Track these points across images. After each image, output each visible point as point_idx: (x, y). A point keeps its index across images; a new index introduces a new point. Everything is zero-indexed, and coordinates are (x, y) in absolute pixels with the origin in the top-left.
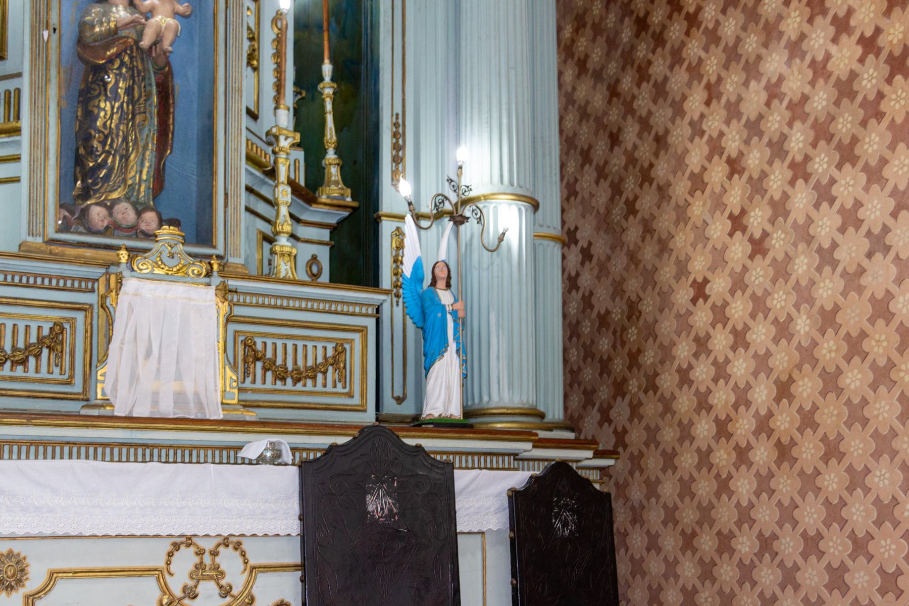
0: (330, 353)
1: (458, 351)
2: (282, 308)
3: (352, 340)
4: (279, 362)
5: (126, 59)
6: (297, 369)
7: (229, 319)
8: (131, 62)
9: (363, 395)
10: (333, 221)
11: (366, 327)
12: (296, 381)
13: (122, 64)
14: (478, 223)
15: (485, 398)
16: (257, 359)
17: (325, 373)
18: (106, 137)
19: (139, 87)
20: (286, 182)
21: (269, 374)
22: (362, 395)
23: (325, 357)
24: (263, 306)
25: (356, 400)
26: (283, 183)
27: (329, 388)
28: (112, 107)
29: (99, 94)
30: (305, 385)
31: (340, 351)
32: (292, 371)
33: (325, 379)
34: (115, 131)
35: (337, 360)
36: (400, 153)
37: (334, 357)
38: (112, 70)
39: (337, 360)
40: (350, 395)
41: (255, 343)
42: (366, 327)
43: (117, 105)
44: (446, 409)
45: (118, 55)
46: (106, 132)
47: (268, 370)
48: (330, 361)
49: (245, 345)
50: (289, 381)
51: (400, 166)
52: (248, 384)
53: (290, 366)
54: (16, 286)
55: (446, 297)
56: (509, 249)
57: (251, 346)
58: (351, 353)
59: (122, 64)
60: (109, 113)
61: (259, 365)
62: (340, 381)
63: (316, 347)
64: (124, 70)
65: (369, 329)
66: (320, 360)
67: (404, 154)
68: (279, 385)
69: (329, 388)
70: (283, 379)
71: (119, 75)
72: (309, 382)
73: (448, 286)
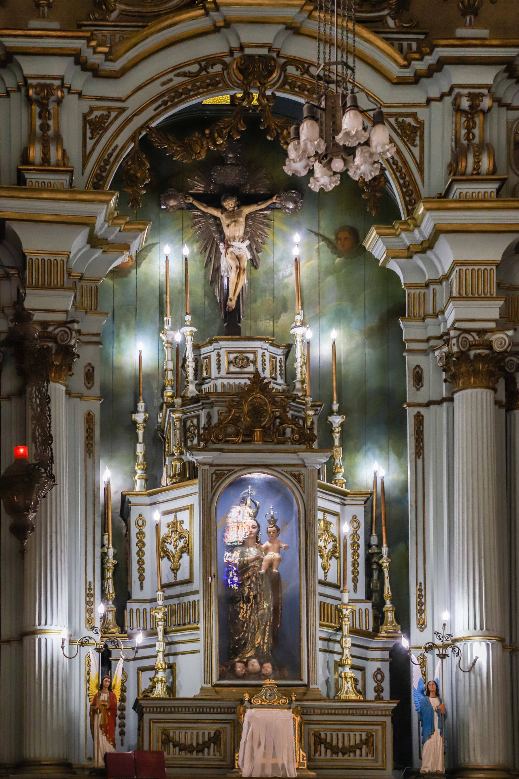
0: (364, 737)
1: (441, 734)
2: (335, 714)
3: (377, 730)
4: (334, 743)
5: (254, 579)
8: (256, 581)
9: (384, 761)
11: (385, 722)
12: (344, 754)
13: (252, 582)
14: (457, 656)
16: (322, 743)
17: (361, 749)
18: (244, 623)
21: (329, 752)
22: (383, 761)
23: (361, 740)
24: (324, 714)
28: (247, 606)
29: (239, 601)
30: (349, 756)
31: (370, 735)
32: (342, 749)
33: (361, 752)
34: (248, 620)
36: (423, 608)
37: (366, 740)
40: (376, 761)
41: (320, 734)
42: (385, 722)
43: (249, 605)
46: (244, 620)
48: (364, 742)
49: (315, 736)
50: (340, 754)
51: (423, 615)
53: (340, 745)
55: (434, 702)
56: (480, 669)
58: (376, 737)
60: (245, 610)
61: (323, 746)
62: (370, 753)
63: (355, 735)
65: (387, 723)
66: (358, 741)
67: (425, 608)
68: (334, 757)
70: (337, 753)
71: (250, 588)
72: (352, 754)
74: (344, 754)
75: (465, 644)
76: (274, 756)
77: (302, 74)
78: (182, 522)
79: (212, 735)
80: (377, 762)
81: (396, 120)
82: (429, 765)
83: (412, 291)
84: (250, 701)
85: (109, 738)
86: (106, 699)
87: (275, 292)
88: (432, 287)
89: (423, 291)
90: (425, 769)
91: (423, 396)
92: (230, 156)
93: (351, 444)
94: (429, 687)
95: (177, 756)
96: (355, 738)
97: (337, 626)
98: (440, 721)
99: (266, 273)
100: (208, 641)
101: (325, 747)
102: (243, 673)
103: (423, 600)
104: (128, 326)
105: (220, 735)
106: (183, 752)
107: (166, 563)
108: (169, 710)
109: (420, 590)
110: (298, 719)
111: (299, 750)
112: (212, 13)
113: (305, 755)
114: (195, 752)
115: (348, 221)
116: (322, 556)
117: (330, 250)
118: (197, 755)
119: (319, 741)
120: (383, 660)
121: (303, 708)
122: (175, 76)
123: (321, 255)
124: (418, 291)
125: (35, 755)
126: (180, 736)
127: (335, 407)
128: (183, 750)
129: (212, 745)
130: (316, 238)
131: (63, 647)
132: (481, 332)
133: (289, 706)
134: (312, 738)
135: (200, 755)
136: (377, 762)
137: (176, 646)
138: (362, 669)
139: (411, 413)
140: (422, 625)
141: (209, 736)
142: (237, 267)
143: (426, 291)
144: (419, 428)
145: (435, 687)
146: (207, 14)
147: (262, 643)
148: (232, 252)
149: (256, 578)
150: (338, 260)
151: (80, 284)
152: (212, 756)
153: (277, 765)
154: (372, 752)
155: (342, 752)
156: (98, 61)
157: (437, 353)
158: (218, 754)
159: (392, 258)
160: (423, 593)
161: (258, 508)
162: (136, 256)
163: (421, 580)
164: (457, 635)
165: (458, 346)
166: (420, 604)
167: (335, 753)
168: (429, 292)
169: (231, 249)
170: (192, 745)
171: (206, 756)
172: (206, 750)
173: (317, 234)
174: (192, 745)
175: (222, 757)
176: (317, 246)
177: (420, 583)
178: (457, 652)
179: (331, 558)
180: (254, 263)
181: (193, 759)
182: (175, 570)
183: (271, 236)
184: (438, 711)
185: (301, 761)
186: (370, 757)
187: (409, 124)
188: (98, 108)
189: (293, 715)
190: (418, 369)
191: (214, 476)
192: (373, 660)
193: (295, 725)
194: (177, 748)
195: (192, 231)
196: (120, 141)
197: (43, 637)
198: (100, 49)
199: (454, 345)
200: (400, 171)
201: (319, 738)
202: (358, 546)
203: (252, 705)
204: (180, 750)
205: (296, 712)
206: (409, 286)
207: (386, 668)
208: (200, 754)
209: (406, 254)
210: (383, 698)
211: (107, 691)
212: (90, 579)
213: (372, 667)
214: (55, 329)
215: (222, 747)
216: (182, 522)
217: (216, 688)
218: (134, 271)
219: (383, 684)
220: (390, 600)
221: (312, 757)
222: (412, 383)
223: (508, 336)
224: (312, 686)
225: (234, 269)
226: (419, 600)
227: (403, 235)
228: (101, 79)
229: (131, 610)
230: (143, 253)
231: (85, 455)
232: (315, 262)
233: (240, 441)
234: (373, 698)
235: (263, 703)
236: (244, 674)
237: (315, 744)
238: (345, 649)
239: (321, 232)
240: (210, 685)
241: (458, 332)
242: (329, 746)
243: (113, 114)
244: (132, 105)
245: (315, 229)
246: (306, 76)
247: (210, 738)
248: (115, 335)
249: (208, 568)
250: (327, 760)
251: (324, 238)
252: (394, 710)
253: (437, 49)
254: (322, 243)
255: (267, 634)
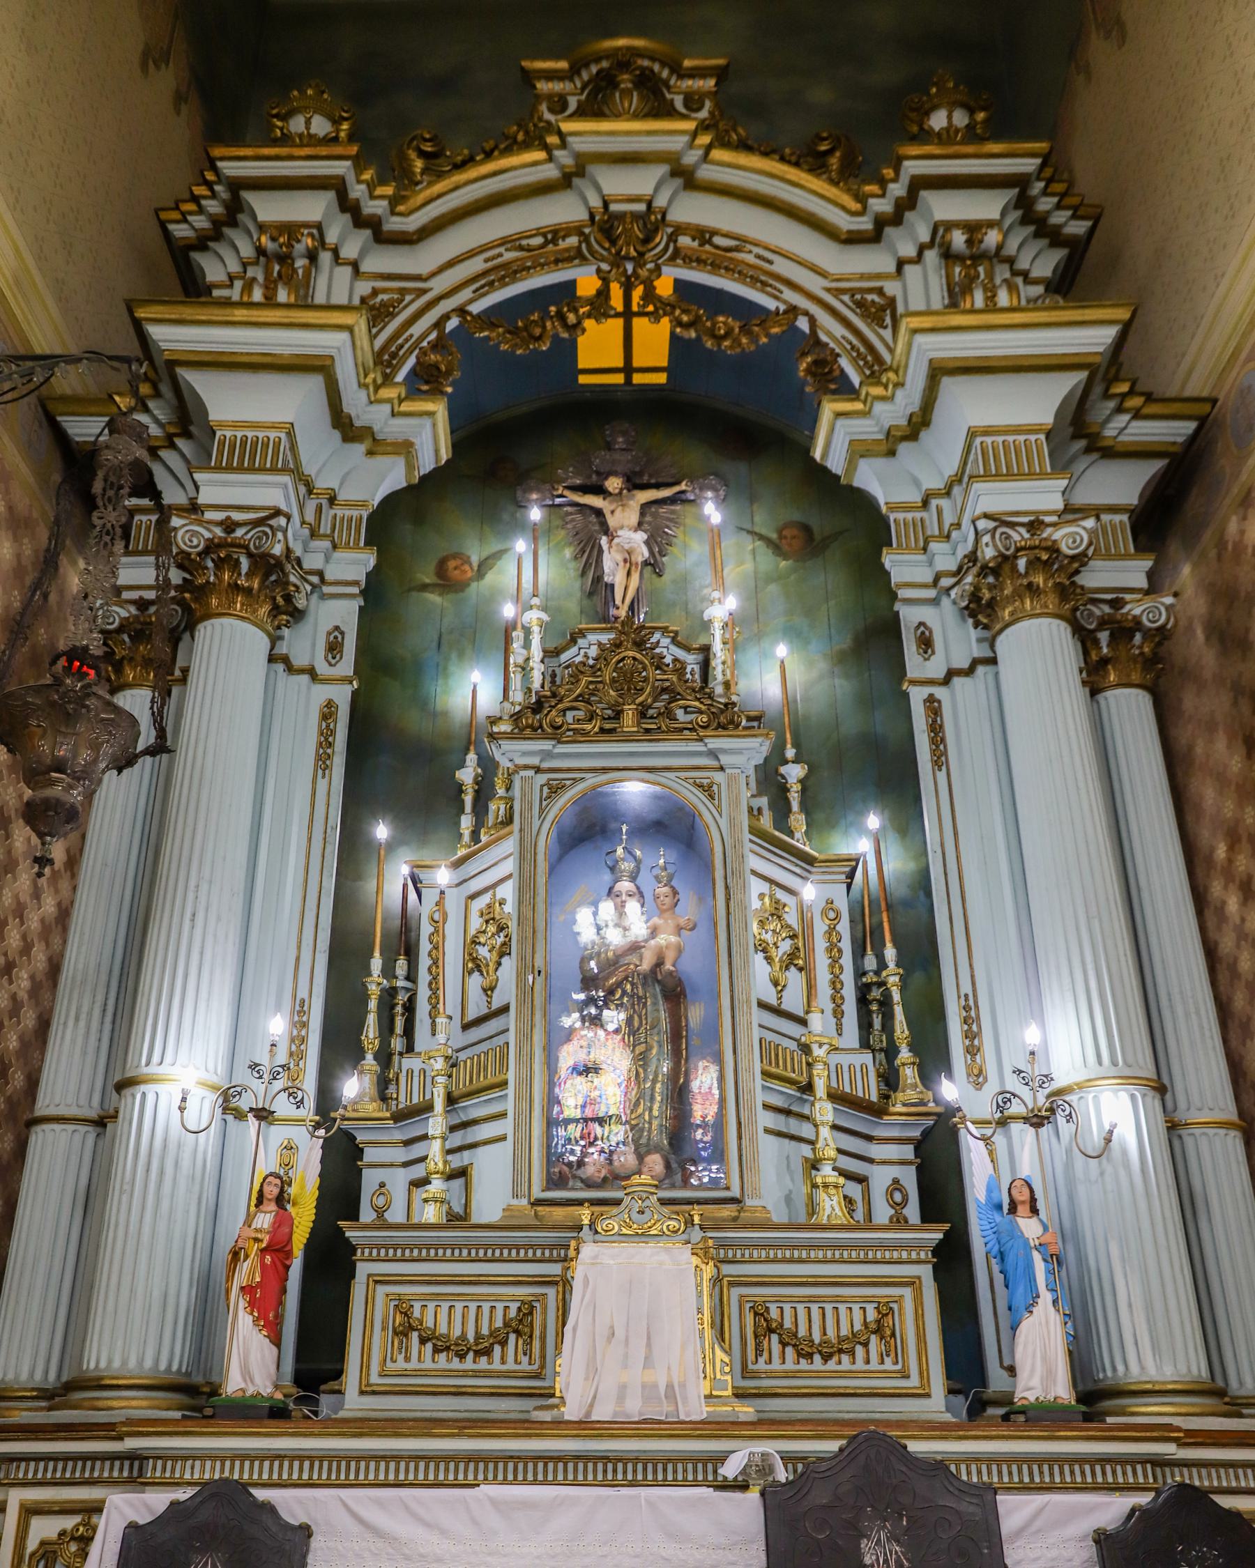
0: (872, 1315)
1: (1055, 1302)
4: (802, 1332)
5: (629, 987)
6: (825, 1342)
7: (717, 1280)
9: (924, 1374)
10: (916, 1133)
11: (919, 1278)
12: (826, 1358)
13: (624, 993)
15: (1121, 1368)
16: (772, 1331)
17: (866, 1345)
19: (640, 1017)
20: (825, 1097)
21: (790, 1351)
22: (921, 1373)
23: (865, 1324)
24: (775, 1261)
25: (914, 1381)
26: (820, 1099)
27: (874, 1365)
30: (840, 1363)
31: (885, 1311)
32: (820, 1345)
33: (868, 1352)
35: (881, 1328)
37: (878, 1321)
38: (612, 1001)
39: (881, 1328)
41: (767, 1309)
42: (919, 1278)
44: (1046, 1391)
45: (619, 984)
47: (788, 1344)
48: (873, 1326)
49: (756, 1314)
50: (817, 1358)
52: (761, 1365)
53: (817, 1338)
54: (480, 1261)
55: (1030, 1228)
57: (762, 1315)
58: (900, 1315)
59: (624, 993)
61: (775, 1338)
62: (888, 1355)
64: (626, 999)
65: (923, 1279)
66: (858, 1326)
69: (874, 1365)
70: (809, 1356)
72: (845, 1358)
73: (1034, 1211)
74: (826, 1358)
75: (1081, 1098)
76: (648, 1362)
77: (701, 245)
78: (502, 902)
79: (513, 1313)
80: (908, 1377)
81: (853, 296)
82: (1036, 1382)
83: (901, 516)
84: (592, 1225)
85: (258, 1319)
86: (266, 1226)
87: (690, 606)
88: (934, 503)
89: (918, 515)
90: (1025, 1394)
91: (936, 667)
92: (620, 440)
93: (819, 816)
94: (1014, 1192)
95: (428, 1364)
96: (851, 1319)
97: (803, 1079)
98: (1050, 1272)
99: (674, 582)
100: (525, 1105)
101: (781, 1342)
102: (602, 1175)
103: (975, 1028)
104: (461, 655)
105: (531, 1313)
106: (443, 1356)
107: (475, 981)
108: (416, 1252)
109: (967, 1008)
110: (709, 1271)
111: (713, 1349)
112: (557, 153)
113: (727, 1360)
114: (471, 1355)
115: (796, 516)
116: (769, 959)
117: (770, 552)
118: (474, 1362)
119: (766, 1327)
120: (903, 1163)
121: (722, 1245)
122: (507, 250)
123: (758, 558)
124: (909, 516)
125: (125, 1362)
126: (436, 1317)
127: (790, 753)
128: (442, 1351)
129: (512, 1337)
130: (750, 538)
131: (182, 1109)
132: (1035, 525)
133: (685, 1237)
134: (749, 1319)
135: (483, 1363)
136: (908, 1377)
137: (476, 1128)
138: (861, 1180)
139: (917, 696)
140: (978, 1076)
141: (505, 1315)
142: (625, 561)
143: (925, 515)
144: (934, 721)
145: (1026, 1191)
146: (551, 159)
147: (647, 1118)
148: (618, 544)
149: (632, 984)
150: (783, 564)
151: (332, 512)
152: (510, 1365)
153: (655, 1386)
154: (893, 1354)
155: (820, 1352)
156: (379, 211)
157: (953, 593)
158: (525, 1360)
159: (862, 456)
160: (973, 1013)
161: (638, 862)
162: (479, 566)
163: (966, 988)
164: (1060, 1081)
165: (995, 546)
166: (971, 1036)
167: (804, 1356)
168: (931, 518)
169: (616, 541)
170: (463, 1337)
171: (497, 1365)
172: (497, 1348)
173: (749, 532)
174: (463, 1337)
175: (536, 1367)
176: (750, 547)
177: (966, 996)
178: (1067, 1112)
179: (787, 968)
180: (653, 565)
181: (465, 1374)
182: (488, 990)
183: (681, 536)
184: (1041, 1247)
185: (718, 1376)
186: (888, 1365)
187: (873, 301)
188: (385, 291)
189: (695, 1260)
190: (922, 629)
191: (546, 790)
192: (884, 1162)
193: (699, 1285)
194: (429, 1346)
195: (563, 533)
196: (417, 330)
197: (149, 1089)
198: (379, 191)
199: (987, 545)
200: (864, 359)
201: (765, 1320)
202: (840, 951)
203: (597, 1237)
204: (436, 1350)
205: (703, 1253)
206: (893, 508)
207: (909, 1178)
208: (484, 1359)
209: (884, 448)
210: (906, 1221)
211: (273, 1207)
212: (303, 993)
213: (881, 1178)
214: (247, 533)
215: (536, 1344)
216: (502, 902)
217: (539, 1208)
218: (474, 585)
219: (905, 1211)
220: (908, 1045)
221: (751, 1366)
222: (914, 648)
223: (1084, 528)
224: (749, 1202)
225: (622, 564)
226: (966, 1027)
227: (879, 407)
228: (391, 247)
229: (410, 1072)
230: (490, 561)
231: (316, 771)
232: (749, 566)
233: (596, 729)
234: (886, 1221)
235: (625, 1231)
236: (605, 1179)
237: (756, 1336)
238: (821, 1128)
239: (757, 529)
240: (524, 1202)
241: (991, 524)
242: (790, 1340)
243: (408, 298)
244: (439, 285)
245: (748, 526)
246: (707, 247)
247: (506, 1324)
248: (440, 668)
249: (529, 957)
250: (787, 1375)
251: (761, 537)
252: (938, 1250)
253: (906, 163)
254: (758, 543)
255: (659, 1098)
